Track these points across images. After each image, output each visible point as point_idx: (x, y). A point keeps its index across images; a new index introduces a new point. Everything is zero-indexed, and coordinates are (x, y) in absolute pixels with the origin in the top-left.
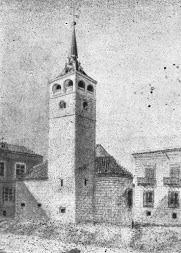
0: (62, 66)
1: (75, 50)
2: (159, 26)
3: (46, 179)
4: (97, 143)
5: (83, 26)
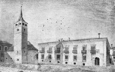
0: (18, 19)
1: (22, 14)
2: (46, 7)
3: (13, 51)
4: (28, 41)
5: (24, 7)
